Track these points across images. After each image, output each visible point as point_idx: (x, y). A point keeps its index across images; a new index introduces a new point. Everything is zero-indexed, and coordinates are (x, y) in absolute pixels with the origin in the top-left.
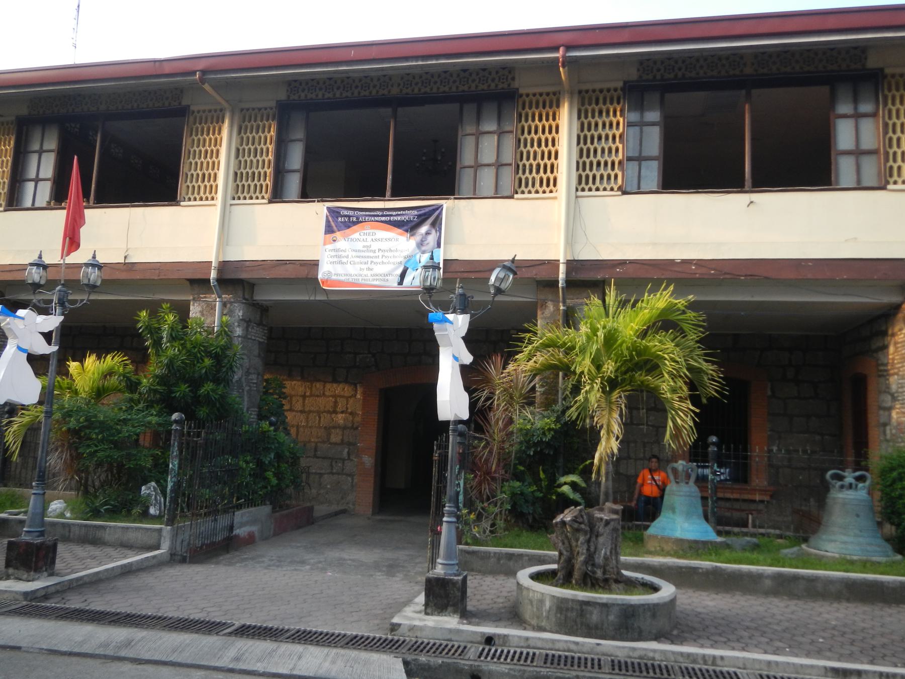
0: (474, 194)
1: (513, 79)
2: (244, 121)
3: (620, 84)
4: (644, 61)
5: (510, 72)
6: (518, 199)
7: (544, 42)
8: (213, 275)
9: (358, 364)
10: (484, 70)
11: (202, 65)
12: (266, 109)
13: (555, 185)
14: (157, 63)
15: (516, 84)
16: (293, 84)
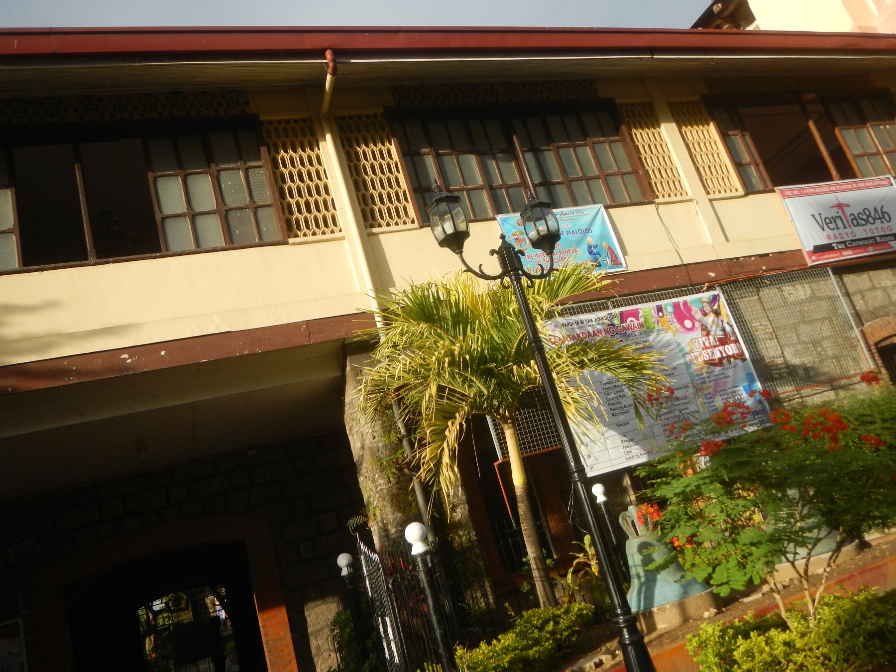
0: (232, 241)
3: (380, 110)
6: (294, 244)
7: (309, 43)
13: (335, 224)
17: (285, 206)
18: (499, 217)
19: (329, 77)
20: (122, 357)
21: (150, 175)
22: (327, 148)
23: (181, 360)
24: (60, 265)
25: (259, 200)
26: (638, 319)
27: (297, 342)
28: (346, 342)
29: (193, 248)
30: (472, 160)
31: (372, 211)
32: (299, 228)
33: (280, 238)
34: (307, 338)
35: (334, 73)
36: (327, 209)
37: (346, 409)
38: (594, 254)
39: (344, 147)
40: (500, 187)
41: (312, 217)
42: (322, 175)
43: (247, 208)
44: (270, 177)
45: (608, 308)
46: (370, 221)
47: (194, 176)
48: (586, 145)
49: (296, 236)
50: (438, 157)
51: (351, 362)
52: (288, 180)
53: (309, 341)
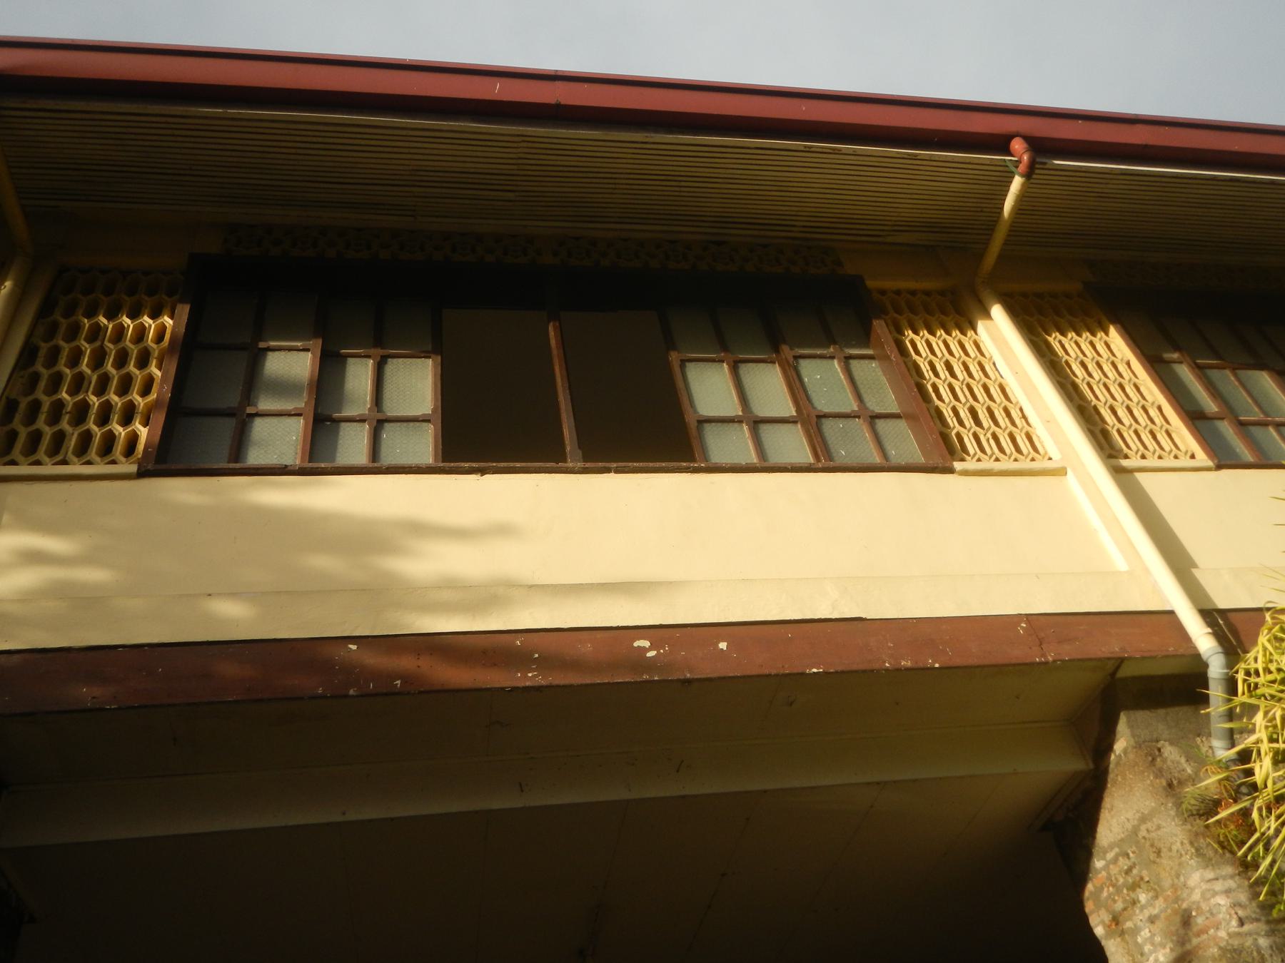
6: (966, 473)
17: (933, 411)
19: (1017, 183)
20: (636, 644)
21: (674, 357)
23: (759, 663)
25: (875, 406)
27: (1017, 654)
28: (1121, 674)
35: (1028, 175)
37: (1098, 864)
41: (989, 435)
43: (855, 417)
47: (750, 365)
49: (963, 460)
51: (1131, 726)
53: (1043, 655)
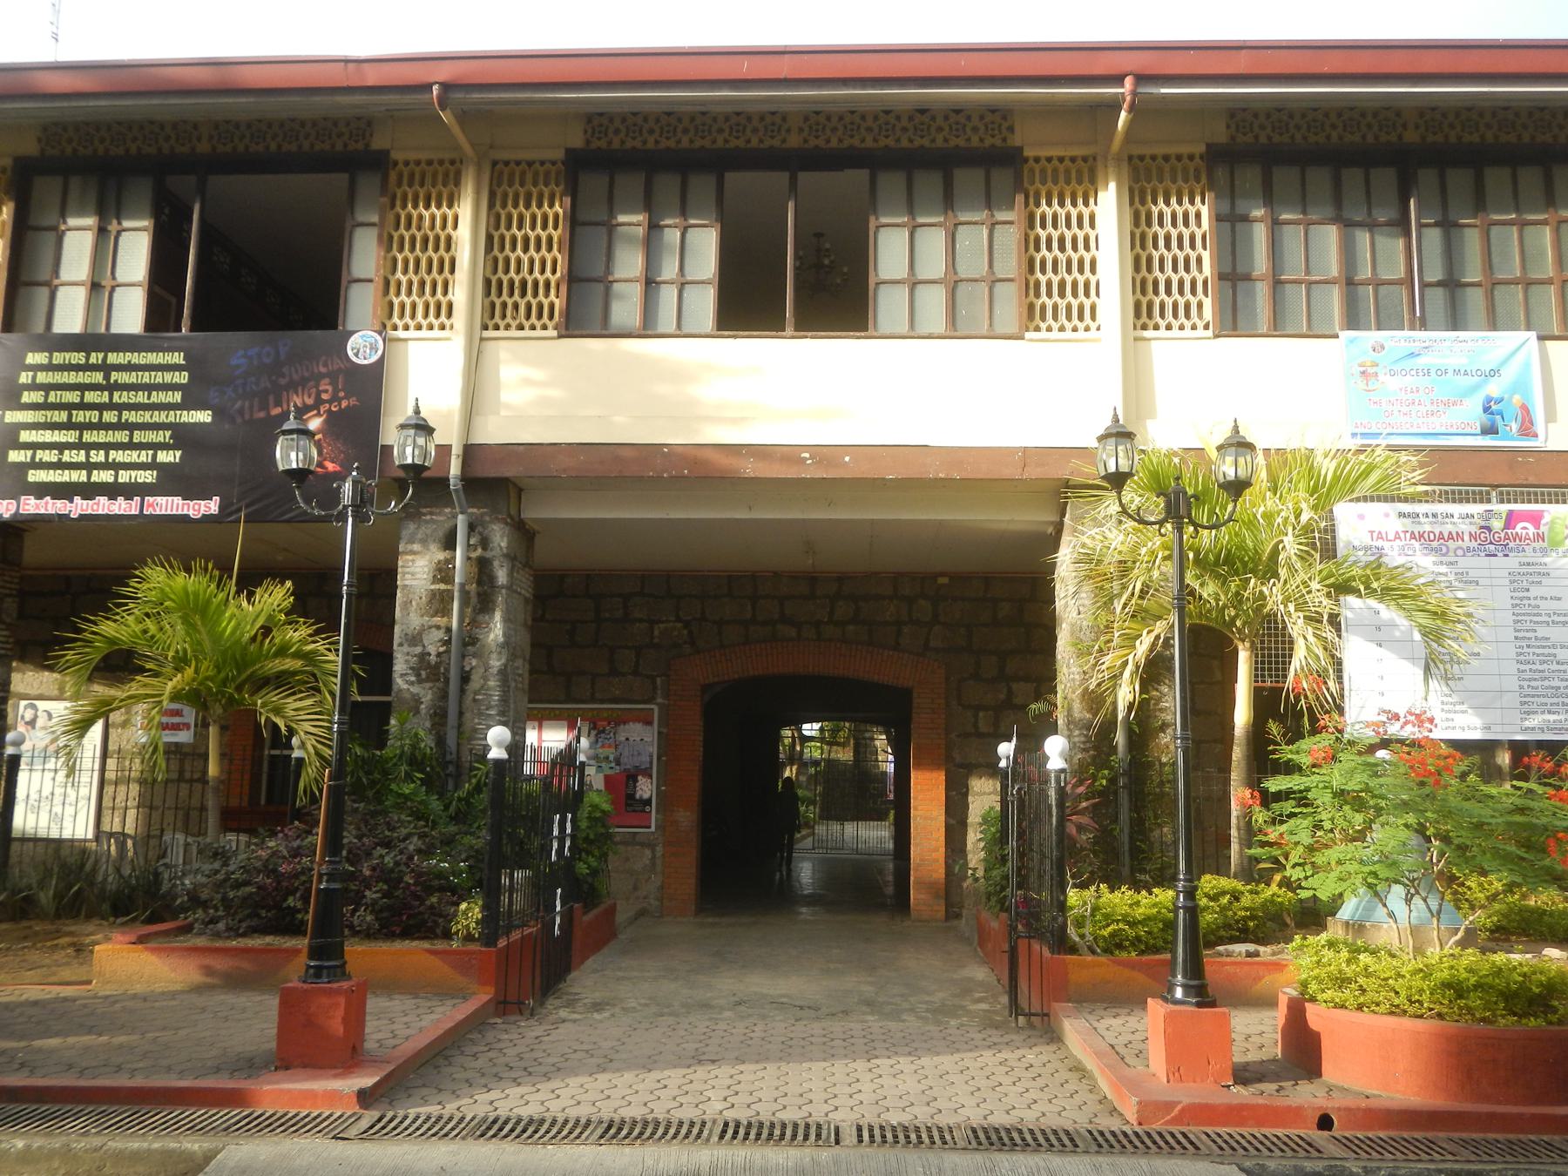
1: (1011, 129)
2: (499, 185)
3: (1200, 149)
4: (1237, 112)
5: (1004, 118)
6: (1031, 340)
7: (1100, 66)
8: (455, 469)
9: (656, 641)
10: (958, 112)
11: (444, 73)
12: (542, 163)
13: (1093, 318)
14: (351, 66)
15: (1016, 140)
16: (596, 119)
18: (1346, 335)
19: (1123, 115)
22: (1108, 203)
23: (864, 471)
24: (755, 333)
26: (1537, 526)
27: (1008, 472)
29: (905, 329)
30: (1330, 235)
31: (1150, 305)
32: (1043, 318)
33: (1014, 330)
34: (1020, 470)
36: (1087, 294)
38: (1492, 413)
39: (1132, 203)
40: (1365, 283)
42: (1092, 244)
44: (1019, 242)
45: (1489, 501)
46: (1144, 318)
48: (1545, 223)
49: (1037, 329)
50: (1276, 224)
52: (1043, 246)
